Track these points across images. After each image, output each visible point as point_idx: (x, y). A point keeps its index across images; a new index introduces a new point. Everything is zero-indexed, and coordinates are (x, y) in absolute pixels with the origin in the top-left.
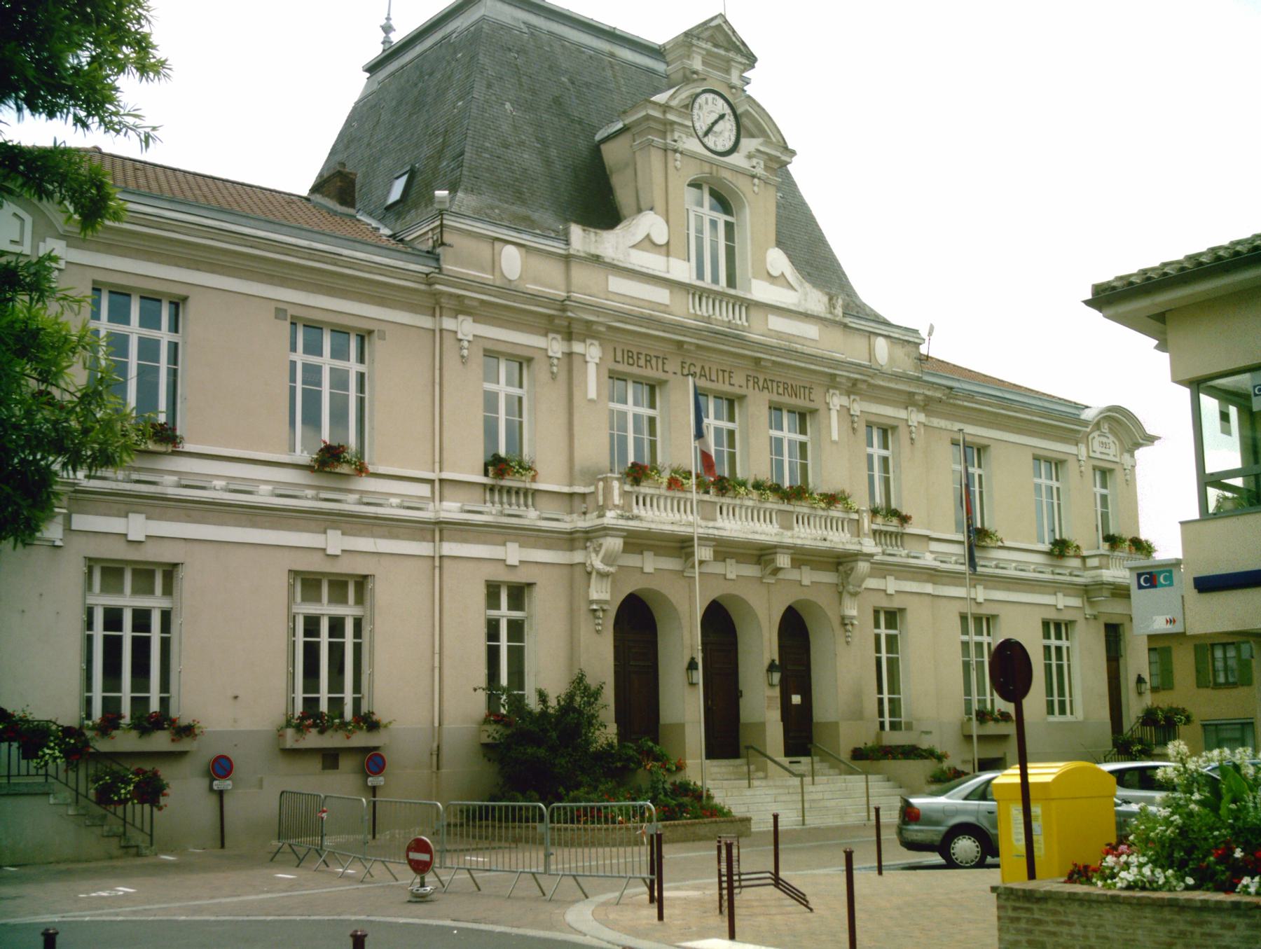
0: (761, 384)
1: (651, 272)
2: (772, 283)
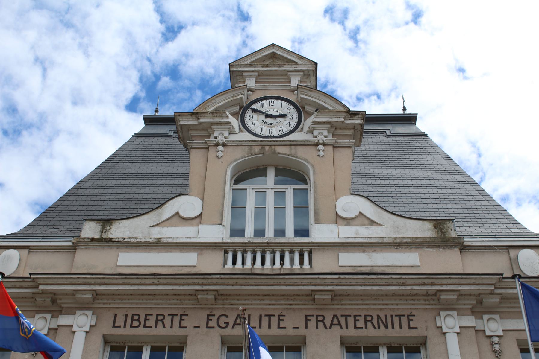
0: (328, 322)
1: (175, 241)
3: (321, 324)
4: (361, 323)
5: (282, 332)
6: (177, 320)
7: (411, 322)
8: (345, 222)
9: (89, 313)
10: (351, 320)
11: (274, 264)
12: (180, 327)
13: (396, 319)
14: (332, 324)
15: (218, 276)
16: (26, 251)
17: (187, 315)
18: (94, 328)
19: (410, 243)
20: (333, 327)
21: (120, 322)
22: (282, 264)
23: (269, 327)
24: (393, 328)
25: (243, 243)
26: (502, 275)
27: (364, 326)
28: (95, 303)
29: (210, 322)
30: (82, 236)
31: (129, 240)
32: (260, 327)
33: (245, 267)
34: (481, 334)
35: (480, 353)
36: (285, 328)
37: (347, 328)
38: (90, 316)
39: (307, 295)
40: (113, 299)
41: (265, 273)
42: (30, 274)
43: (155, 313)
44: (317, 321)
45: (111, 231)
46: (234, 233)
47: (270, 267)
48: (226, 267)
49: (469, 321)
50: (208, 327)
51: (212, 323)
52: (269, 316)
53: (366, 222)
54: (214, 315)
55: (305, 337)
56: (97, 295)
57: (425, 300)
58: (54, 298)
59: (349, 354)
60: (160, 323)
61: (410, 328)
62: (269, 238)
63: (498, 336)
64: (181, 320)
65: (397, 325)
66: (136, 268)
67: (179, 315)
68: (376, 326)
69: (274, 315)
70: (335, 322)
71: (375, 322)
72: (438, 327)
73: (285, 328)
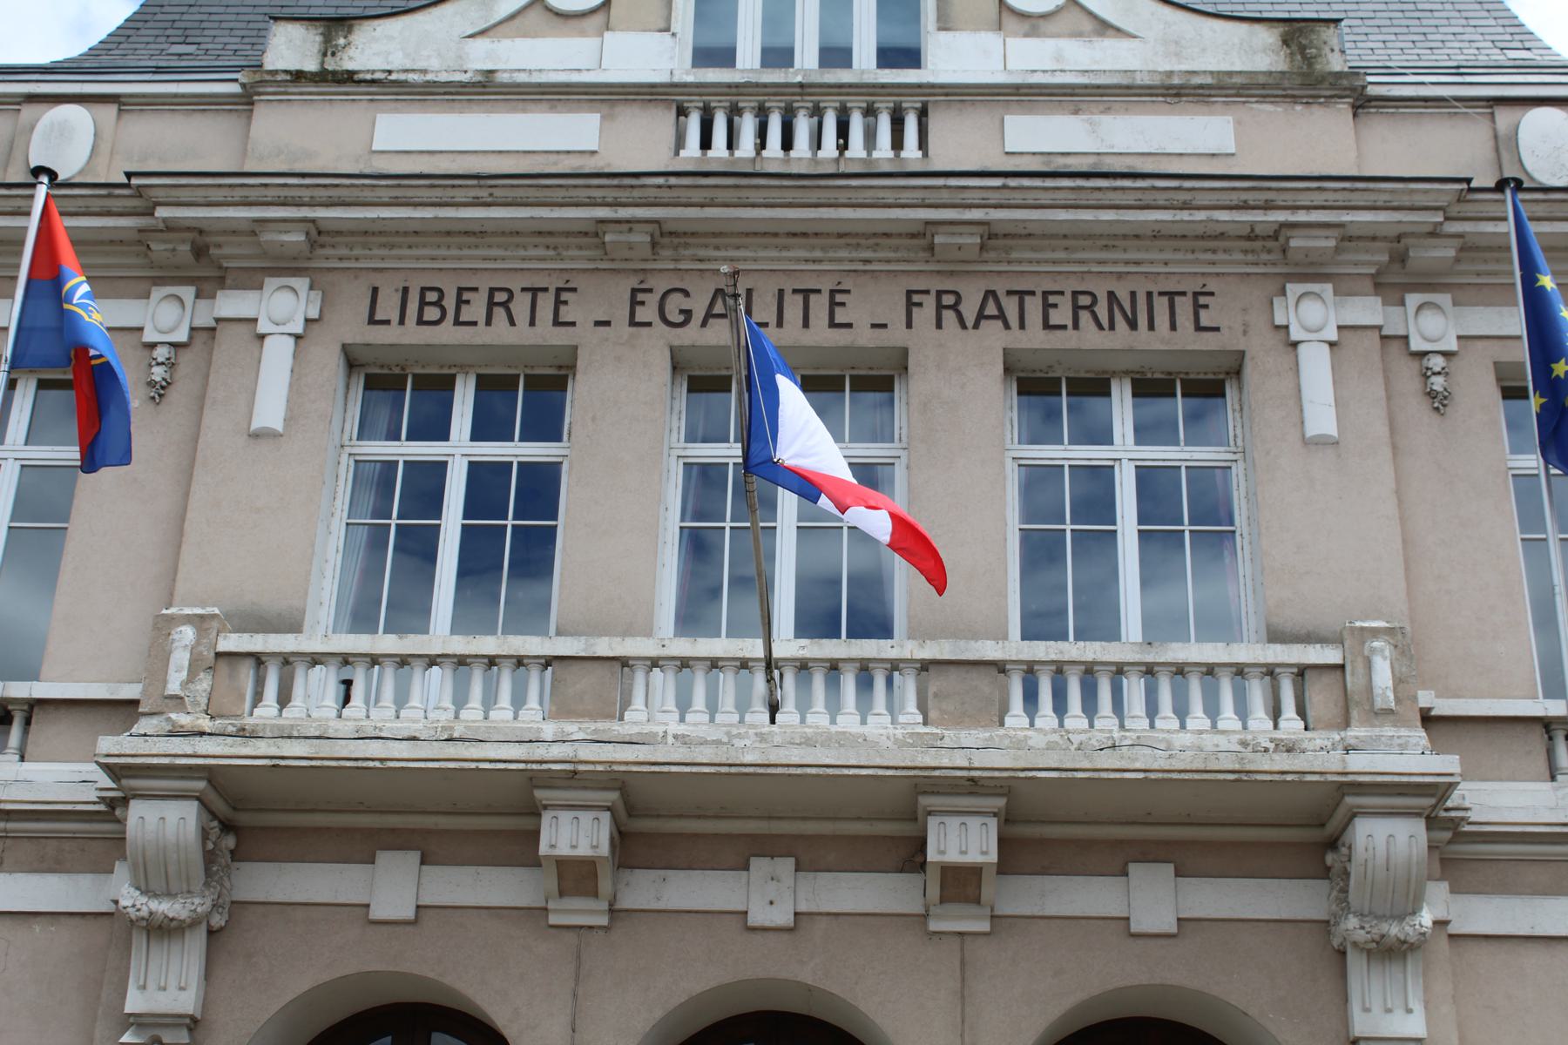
0: (969, 310)
2: (1033, 33)
3: (949, 316)
4: (1061, 315)
5: (840, 338)
6: (546, 304)
7: (1203, 313)
8: (1026, 26)
9: (301, 283)
10: (1034, 306)
11: (819, 147)
12: (557, 322)
13: (1161, 304)
14: (981, 316)
15: (661, 181)
16: (110, 111)
17: (574, 290)
18: (315, 326)
19: (1209, 87)
20: (983, 323)
21: (388, 307)
22: (843, 147)
23: (806, 324)
24: (1151, 327)
25: (729, 86)
26: (1468, 181)
27: (1070, 323)
28: (313, 256)
29: (638, 309)
30: (268, 66)
31: (402, 77)
32: (780, 324)
33: (738, 154)
34: (1395, 347)
35: (1389, 398)
36: (849, 326)
37: (1022, 326)
38: (303, 293)
39: (913, 236)
40: (365, 246)
41: (795, 171)
42: (129, 175)
43: (485, 283)
44: (940, 307)
45: (351, 52)
46: (705, 56)
47: (809, 155)
48: (683, 153)
49: (1367, 310)
50: (633, 323)
51: (646, 313)
52: (806, 293)
53: (1087, 25)
54: (650, 291)
55: (905, 352)
56: (319, 233)
57: (1245, 252)
58: (201, 242)
59: (1025, 398)
60: (500, 313)
61: (1199, 328)
62: (806, 72)
63: (1446, 354)
64: (559, 302)
65: (1162, 319)
66: (426, 157)
67: (552, 291)
68: (1105, 323)
69: (819, 291)
70: (991, 311)
71: (1102, 311)
72: (1278, 327)
73: (849, 326)
